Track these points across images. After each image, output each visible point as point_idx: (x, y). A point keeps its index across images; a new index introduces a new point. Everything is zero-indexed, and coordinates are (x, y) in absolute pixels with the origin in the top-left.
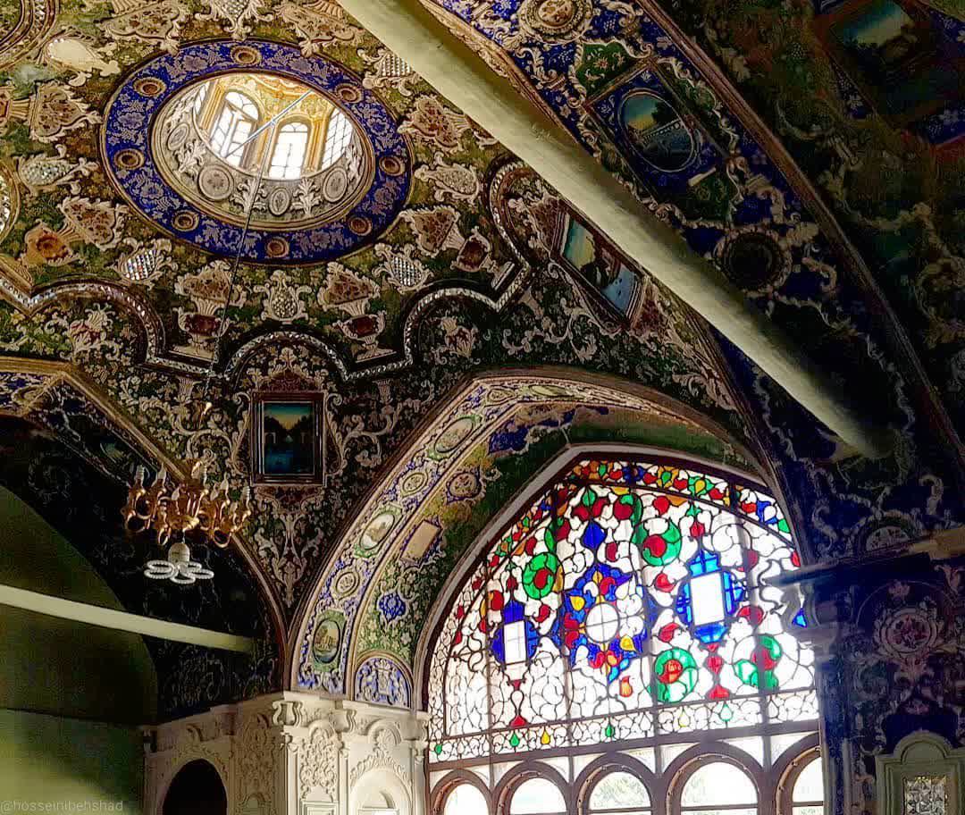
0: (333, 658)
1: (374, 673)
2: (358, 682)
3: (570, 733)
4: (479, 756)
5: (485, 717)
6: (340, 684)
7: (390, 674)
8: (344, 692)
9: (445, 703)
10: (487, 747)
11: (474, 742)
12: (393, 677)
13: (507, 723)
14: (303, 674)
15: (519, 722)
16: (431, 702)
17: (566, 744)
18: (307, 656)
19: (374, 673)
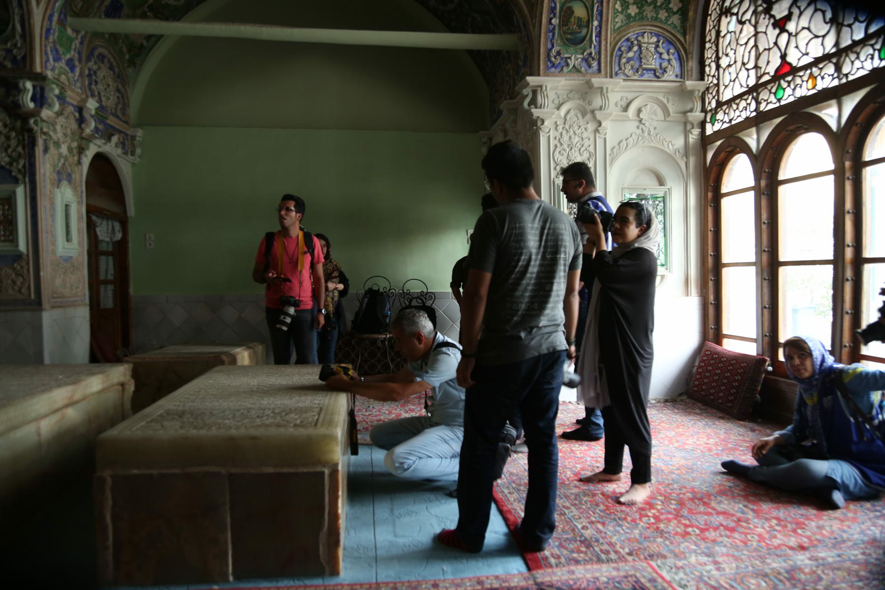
0: (584, 39)
1: (636, 48)
2: (615, 59)
3: (838, 68)
4: (747, 118)
5: (752, 73)
6: (595, 64)
7: (657, 46)
8: (599, 70)
9: (718, 67)
10: (753, 105)
11: (743, 104)
12: (661, 50)
13: (772, 73)
14: (553, 59)
15: (786, 71)
16: (707, 69)
17: (836, 83)
18: (554, 41)
19: (636, 48)
